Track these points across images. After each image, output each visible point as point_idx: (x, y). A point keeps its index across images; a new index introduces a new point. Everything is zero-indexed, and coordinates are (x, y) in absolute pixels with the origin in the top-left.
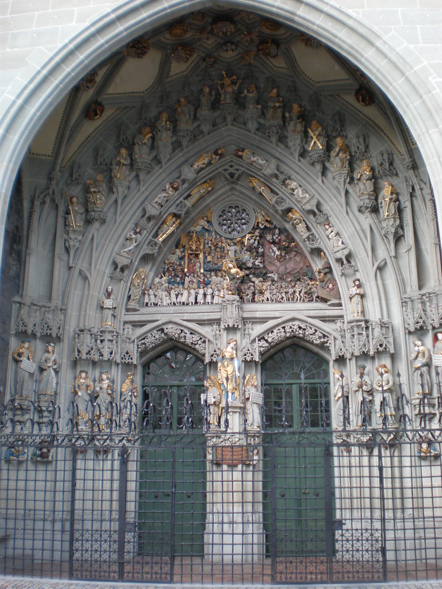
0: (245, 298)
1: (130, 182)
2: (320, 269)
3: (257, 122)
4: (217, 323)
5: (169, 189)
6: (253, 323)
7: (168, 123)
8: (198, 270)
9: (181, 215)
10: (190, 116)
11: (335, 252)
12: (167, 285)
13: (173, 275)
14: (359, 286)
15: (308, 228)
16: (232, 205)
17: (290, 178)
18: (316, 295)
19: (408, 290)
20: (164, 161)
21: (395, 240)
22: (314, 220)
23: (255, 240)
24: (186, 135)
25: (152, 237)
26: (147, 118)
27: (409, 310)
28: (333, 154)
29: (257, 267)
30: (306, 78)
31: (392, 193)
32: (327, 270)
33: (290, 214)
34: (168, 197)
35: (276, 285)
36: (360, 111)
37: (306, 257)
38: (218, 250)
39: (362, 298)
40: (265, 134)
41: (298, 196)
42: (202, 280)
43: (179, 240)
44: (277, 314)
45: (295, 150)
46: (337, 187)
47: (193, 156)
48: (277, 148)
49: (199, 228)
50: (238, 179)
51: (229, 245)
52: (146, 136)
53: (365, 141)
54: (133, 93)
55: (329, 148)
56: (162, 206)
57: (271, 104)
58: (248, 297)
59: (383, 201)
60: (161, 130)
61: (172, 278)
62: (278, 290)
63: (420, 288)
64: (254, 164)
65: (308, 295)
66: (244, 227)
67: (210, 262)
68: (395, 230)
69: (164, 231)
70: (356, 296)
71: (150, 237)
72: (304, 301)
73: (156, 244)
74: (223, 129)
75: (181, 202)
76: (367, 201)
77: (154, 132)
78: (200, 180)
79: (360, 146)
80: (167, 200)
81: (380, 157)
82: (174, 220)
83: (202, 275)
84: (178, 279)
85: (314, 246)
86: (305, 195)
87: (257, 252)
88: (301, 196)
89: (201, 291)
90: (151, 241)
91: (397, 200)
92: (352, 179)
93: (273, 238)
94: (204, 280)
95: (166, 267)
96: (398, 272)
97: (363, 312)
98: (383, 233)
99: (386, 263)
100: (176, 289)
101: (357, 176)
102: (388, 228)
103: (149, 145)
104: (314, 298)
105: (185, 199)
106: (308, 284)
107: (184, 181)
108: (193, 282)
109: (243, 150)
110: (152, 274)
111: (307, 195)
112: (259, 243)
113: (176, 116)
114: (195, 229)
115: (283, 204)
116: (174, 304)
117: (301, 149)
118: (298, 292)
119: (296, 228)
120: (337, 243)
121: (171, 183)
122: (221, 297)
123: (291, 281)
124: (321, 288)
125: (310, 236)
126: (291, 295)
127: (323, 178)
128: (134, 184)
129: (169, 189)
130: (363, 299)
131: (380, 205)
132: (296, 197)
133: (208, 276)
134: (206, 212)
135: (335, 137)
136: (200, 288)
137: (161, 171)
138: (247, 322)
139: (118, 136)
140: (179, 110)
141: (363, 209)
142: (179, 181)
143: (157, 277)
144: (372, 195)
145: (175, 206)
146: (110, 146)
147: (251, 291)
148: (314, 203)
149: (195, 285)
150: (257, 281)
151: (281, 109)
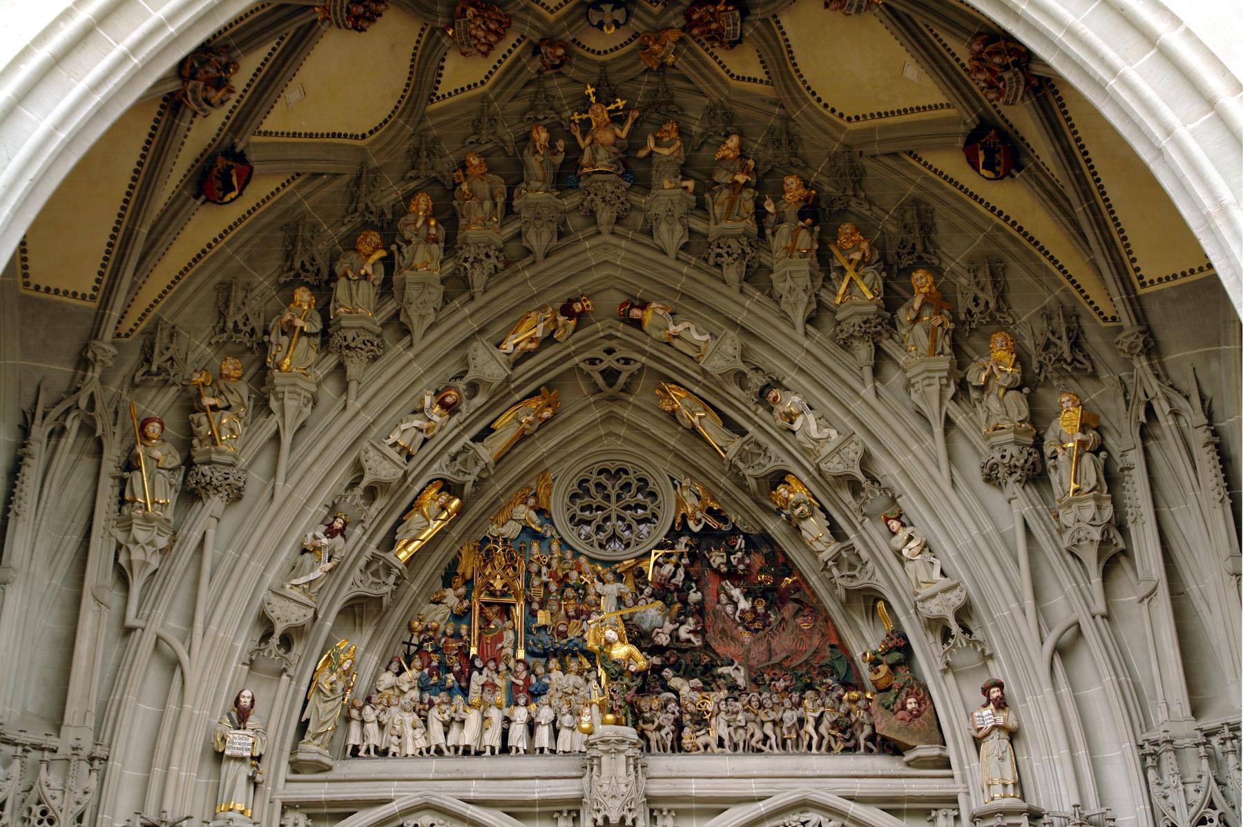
0: (653, 736)
1: (318, 385)
2: (875, 653)
3: (683, 225)
4: (569, 812)
5: (432, 407)
6: (679, 814)
7: (433, 223)
8: (509, 651)
9: (462, 485)
10: (495, 205)
11: (923, 600)
12: (415, 694)
13: (435, 664)
14: (1001, 704)
15: (835, 531)
16: (608, 465)
17: (778, 384)
18: (867, 730)
19: (1159, 716)
20: (418, 329)
21: (1102, 565)
22: (854, 504)
23: (677, 566)
24: (482, 257)
25: (378, 548)
26: (373, 209)
27: (1168, 780)
28: (904, 315)
29: (685, 645)
30: (820, 107)
31: (1083, 428)
32: (896, 656)
33: (782, 490)
34: (428, 430)
35: (745, 699)
36: (976, 198)
37: (828, 619)
38: (569, 592)
39: (1011, 741)
40: (706, 260)
41: (807, 435)
42: (520, 683)
43: (455, 563)
44: (753, 788)
45: (794, 305)
46: (920, 414)
47: (502, 316)
48: (741, 299)
49: (511, 530)
50: (627, 389)
51: (601, 580)
52: (369, 256)
53: (995, 284)
54: (334, 135)
55: (891, 301)
56: (409, 457)
57: (722, 177)
58: (663, 732)
59: (1059, 450)
60: (414, 240)
61: (431, 675)
62: (752, 716)
63: (1196, 712)
64: (676, 343)
65: (843, 732)
66: (644, 528)
67: (545, 627)
68: (1103, 534)
69: (414, 533)
70: (995, 734)
71: (372, 547)
72: (830, 749)
73: (388, 568)
74: (588, 244)
75: (465, 449)
76: (1012, 450)
77: (394, 247)
78: (518, 389)
79: (980, 295)
80: (425, 441)
81: (1041, 325)
82: (444, 497)
83: (521, 667)
84: (451, 677)
85: (854, 584)
86: (826, 430)
87: (685, 602)
88: (815, 435)
89: (521, 714)
90: (375, 558)
91: (1100, 448)
92: (963, 386)
93: (729, 560)
94: (527, 680)
95: (415, 641)
96: (1121, 660)
97: (1019, 784)
98: (1065, 543)
99: (1079, 632)
100: (444, 707)
101: (976, 376)
102: (1079, 529)
103: (377, 283)
104: (862, 742)
105: (478, 438)
106: (840, 699)
107: (474, 388)
108: (495, 686)
109: (644, 306)
110: (373, 660)
111: (833, 433)
112: (688, 576)
113: (455, 203)
114: (502, 530)
115: (761, 460)
116: (439, 751)
117: (809, 303)
118: (811, 720)
119: (798, 528)
120: (929, 574)
121: (437, 393)
122: (584, 731)
123: (786, 688)
124: (882, 710)
125: (844, 554)
126: (789, 729)
127: (878, 384)
128: (329, 390)
129: (432, 407)
130: (1016, 743)
131: (1050, 463)
132: (799, 436)
133: (540, 670)
134: (533, 484)
135: (908, 272)
136: (517, 704)
137: (410, 355)
138: (661, 811)
139: (289, 256)
140: (465, 187)
141: (1002, 472)
142: (461, 384)
143: (387, 669)
144: (1026, 432)
145: (445, 458)
146: (264, 282)
147: (671, 717)
148: (852, 455)
149: (501, 697)
150: (685, 687)
151: (752, 190)
